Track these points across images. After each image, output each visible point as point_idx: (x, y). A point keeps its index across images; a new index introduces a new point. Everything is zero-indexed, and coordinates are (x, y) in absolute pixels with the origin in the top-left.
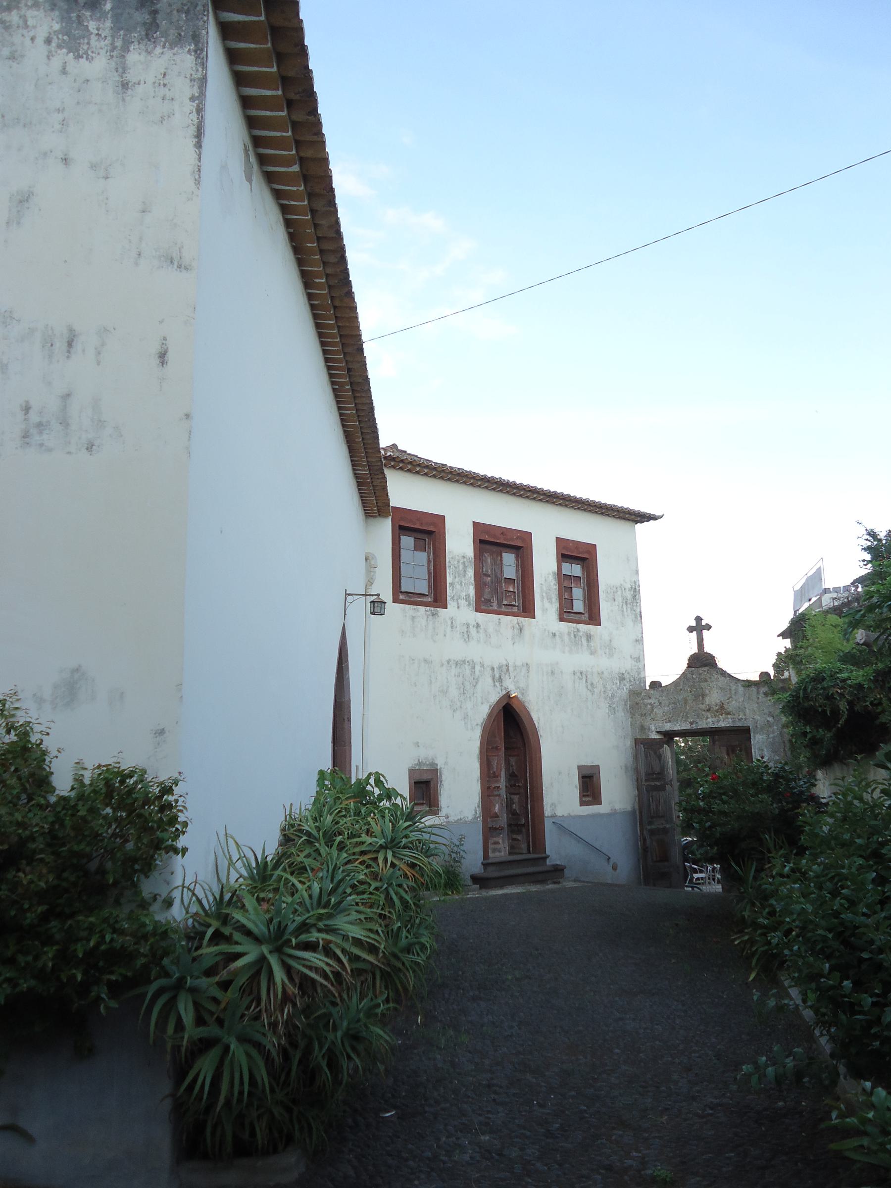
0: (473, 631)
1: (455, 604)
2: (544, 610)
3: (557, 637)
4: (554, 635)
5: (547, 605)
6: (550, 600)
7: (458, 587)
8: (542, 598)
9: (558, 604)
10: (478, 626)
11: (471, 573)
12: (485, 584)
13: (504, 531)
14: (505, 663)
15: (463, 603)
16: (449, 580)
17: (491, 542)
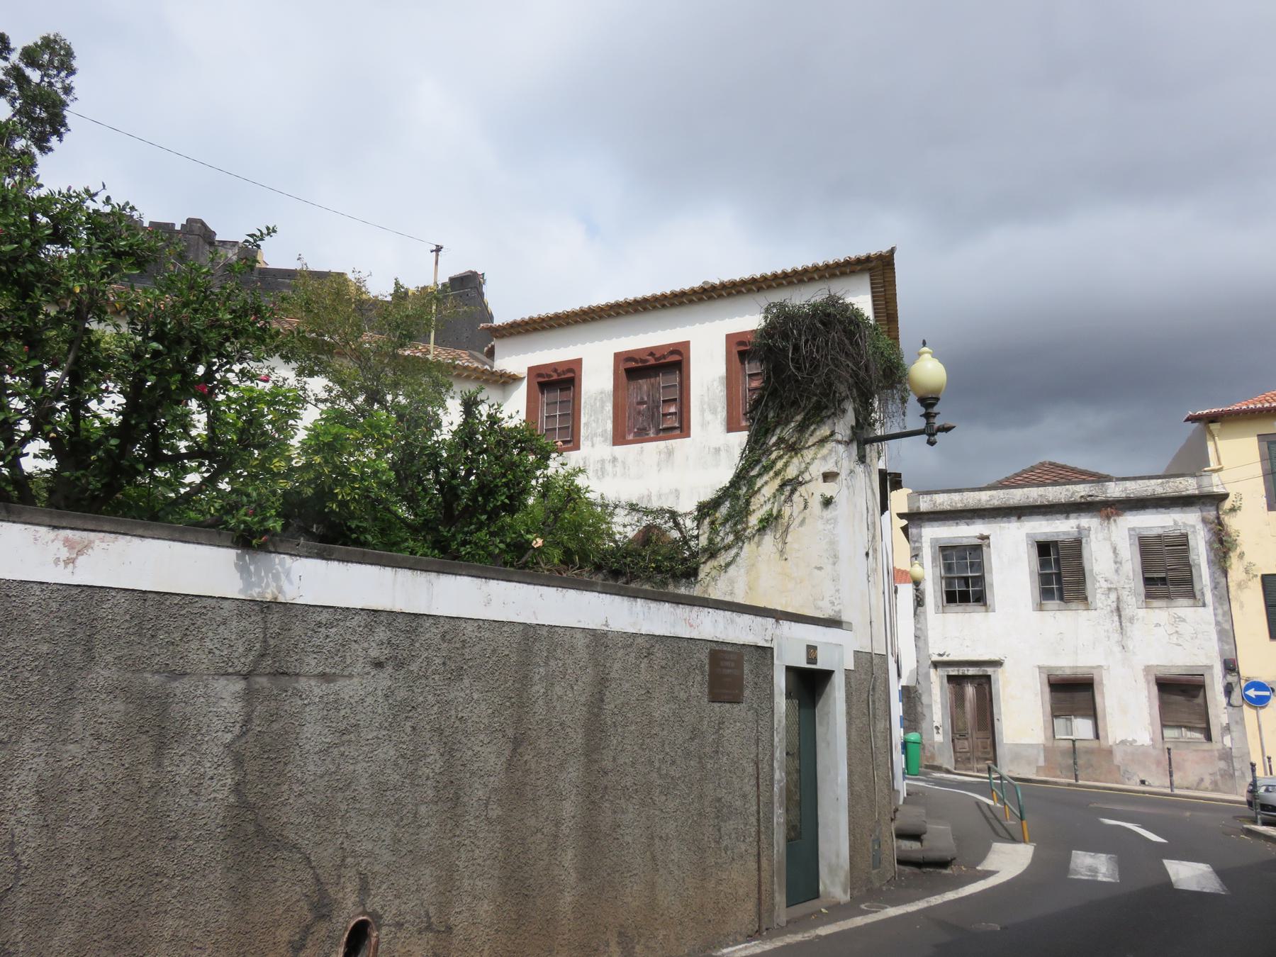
0: (609, 467)
1: (589, 443)
2: (704, 425)
3: (723, 453)
4: (718, 450)
5: (709, 417)
6: (714, 412)
7: (594, 425)
8: (703, 411)
9: (724, 414)
10: (614, 460)
11: (609, 407)
12: (639, 413)
13: (651, 352)
14: (646, 493)
15: (598, 440)
16: (583, 420)
17: (634, 369)
